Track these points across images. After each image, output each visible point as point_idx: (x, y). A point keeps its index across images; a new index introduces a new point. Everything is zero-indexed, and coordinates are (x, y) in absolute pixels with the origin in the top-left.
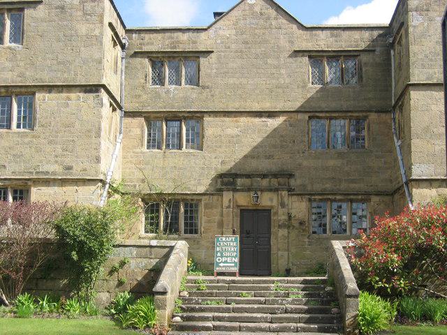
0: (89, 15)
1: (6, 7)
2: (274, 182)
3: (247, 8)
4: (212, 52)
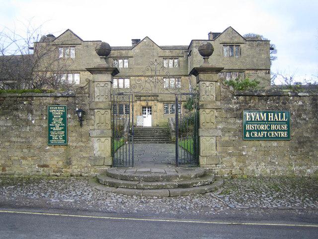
2: (153, 98)
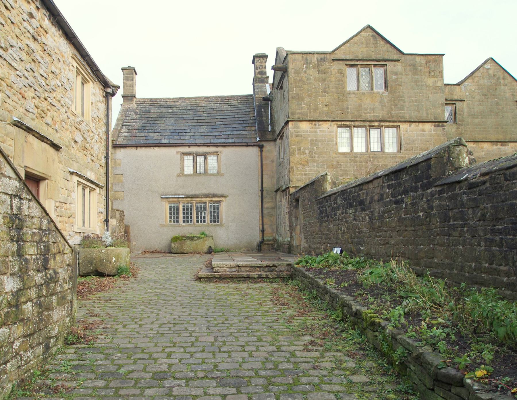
0: (433, 71)
1: (373, 63)
3: (485, 71)
4: (464, 100)
